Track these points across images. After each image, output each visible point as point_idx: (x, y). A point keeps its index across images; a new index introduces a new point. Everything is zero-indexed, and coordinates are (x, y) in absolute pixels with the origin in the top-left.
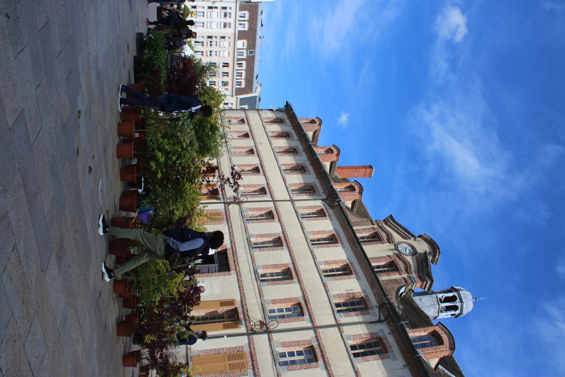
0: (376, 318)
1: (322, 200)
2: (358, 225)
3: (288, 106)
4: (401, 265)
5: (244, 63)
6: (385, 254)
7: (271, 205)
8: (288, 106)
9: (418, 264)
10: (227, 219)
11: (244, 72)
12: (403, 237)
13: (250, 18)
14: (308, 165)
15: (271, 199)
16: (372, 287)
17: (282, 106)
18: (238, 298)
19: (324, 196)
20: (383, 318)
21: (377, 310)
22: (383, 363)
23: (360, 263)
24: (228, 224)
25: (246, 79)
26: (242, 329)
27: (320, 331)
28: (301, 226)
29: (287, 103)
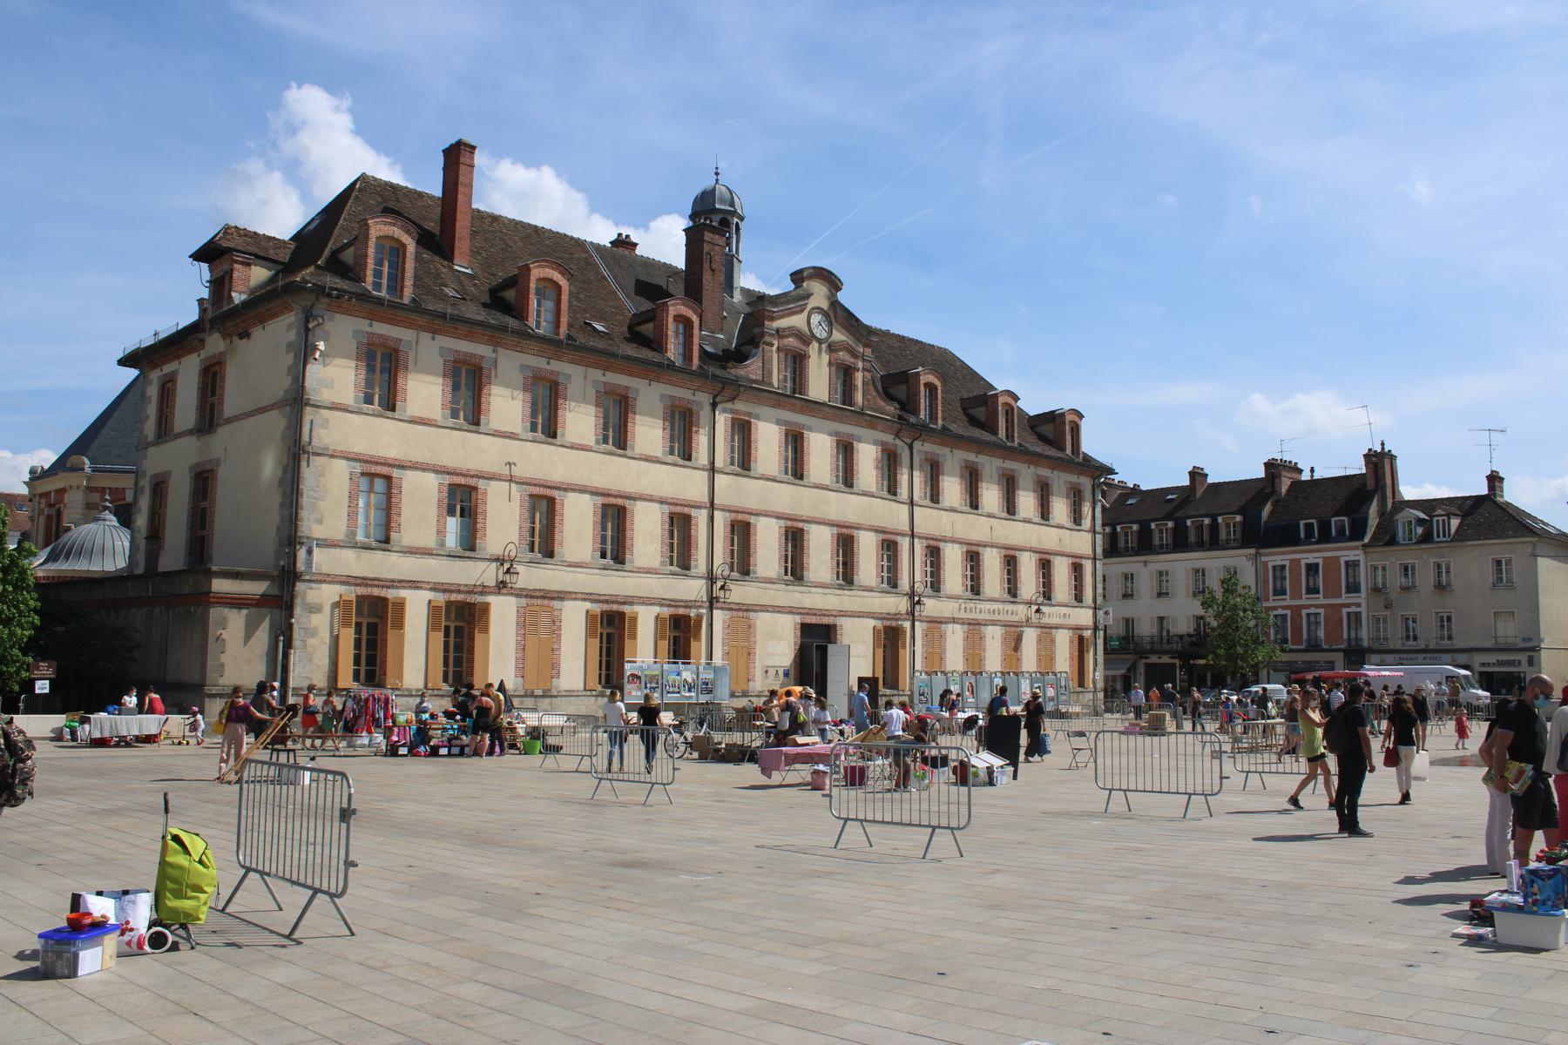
1: (714, 406)
2: (770, 373)
4: (843, 356)
6: (826, 370)
7: (720, 518)
9: (847, 329)
16: (873, 428)
18: (872, 623)
19: (704, 399)
21: (898, 442)
23: (840, 421)
26: (907, 625)
28: (768, 479)
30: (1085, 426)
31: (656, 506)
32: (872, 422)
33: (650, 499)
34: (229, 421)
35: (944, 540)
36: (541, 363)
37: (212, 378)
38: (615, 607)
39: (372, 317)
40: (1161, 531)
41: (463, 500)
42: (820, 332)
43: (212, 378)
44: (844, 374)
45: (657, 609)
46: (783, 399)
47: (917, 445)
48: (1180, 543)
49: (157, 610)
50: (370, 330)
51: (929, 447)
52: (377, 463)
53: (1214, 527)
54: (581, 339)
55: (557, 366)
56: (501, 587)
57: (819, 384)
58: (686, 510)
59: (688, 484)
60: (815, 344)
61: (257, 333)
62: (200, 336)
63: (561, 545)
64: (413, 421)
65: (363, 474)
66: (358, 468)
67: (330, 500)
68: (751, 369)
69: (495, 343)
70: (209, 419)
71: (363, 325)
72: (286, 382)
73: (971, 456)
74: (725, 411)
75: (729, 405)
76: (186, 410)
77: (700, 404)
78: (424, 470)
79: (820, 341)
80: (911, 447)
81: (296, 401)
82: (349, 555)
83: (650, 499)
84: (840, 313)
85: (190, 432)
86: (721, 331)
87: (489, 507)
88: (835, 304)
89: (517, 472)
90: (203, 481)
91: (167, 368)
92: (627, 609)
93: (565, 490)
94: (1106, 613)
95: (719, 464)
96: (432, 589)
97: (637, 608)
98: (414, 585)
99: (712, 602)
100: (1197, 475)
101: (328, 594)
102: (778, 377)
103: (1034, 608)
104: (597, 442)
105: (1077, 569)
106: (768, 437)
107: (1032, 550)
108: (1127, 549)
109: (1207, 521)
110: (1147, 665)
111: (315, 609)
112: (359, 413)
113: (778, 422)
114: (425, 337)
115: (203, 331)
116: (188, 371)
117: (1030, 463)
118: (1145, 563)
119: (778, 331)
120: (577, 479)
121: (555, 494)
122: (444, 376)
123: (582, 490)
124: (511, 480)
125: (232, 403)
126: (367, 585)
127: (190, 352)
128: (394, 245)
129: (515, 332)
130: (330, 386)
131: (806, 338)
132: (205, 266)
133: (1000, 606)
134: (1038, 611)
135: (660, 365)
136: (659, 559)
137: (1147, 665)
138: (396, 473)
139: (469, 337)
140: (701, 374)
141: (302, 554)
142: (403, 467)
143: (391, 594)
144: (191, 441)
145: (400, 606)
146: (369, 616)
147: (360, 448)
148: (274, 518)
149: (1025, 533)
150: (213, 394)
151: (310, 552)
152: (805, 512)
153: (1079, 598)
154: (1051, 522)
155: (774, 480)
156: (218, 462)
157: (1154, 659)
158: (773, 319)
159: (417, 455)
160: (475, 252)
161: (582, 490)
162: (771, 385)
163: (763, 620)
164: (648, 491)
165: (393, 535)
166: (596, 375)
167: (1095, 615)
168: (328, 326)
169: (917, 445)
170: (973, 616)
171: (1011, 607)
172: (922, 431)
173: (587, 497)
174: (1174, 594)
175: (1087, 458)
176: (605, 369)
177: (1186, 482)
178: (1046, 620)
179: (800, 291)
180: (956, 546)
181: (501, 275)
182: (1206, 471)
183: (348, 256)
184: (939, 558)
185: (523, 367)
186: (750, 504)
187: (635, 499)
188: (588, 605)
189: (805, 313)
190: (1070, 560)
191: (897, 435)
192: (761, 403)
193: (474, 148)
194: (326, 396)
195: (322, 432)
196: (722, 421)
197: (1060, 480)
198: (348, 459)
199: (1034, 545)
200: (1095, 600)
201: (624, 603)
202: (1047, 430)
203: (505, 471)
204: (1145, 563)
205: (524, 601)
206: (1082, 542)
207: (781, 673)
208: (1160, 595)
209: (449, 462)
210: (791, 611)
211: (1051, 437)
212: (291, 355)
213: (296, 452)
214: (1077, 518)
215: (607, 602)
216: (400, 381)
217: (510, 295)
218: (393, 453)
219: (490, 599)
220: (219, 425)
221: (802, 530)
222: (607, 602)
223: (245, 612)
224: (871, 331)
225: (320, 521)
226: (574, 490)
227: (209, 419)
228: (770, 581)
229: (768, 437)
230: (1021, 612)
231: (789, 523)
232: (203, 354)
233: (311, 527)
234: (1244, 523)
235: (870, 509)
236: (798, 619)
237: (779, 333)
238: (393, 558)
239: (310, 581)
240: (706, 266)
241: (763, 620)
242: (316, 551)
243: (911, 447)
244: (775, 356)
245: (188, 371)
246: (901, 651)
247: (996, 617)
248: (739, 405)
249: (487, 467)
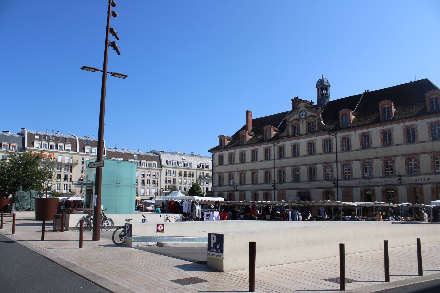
0: (334, 138)
2: (289, 133)
3: (210, 151)
5: (142, 161)
6: (305, 125)
8: (210, 151)
11: (148, 162)
13: (115, 157)
15: (273, 169)
17: (210, 154)
18: (322, 190)
20: (334, 135)
21: (331, 136)
25: (152, 161)
27: (338, 160)
29: (209, 151)
33: (261, 169)
35: (352, 161)
45: (263, 192)
56: (237, 191)
60: (301, 120)
68: (285, 134)
73: (365, 131)
77: (271, 147)
80: (336, 136)
89: (239, 170)
107: (401, 155)
124: (237, 171)
131: (298, 120)
155: (290, 158)
158: (289, 120)
163: (288, 192)
180: (358, 162)
189: (298, 114)
191: (329, 135)
236: (297, 191)
243: (336, 136)
249: (234, 170)
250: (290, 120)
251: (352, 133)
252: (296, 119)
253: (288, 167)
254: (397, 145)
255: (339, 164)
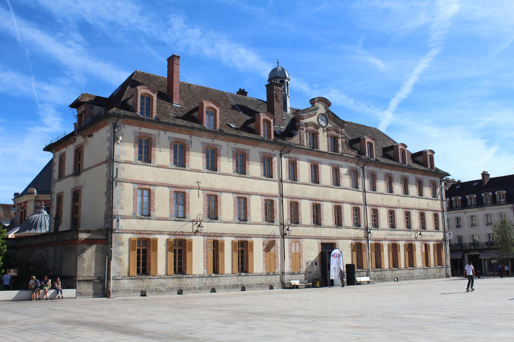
1: (281, 155)
2: (303, 141)
4: (334, 133)
10: (298, 238)
12: (315, 115)
14: (235, 146)
16: (347, 161)
19: (277, 152)
21: (358, 167)
22: (380, 180)
24: (302, 238)
28: (305, 184)
30: (435, 156)
31: (259, 197)
32: (347, 159)
34: (86, 170)
36: (209, 141)
37: (79, 154)
38: (244, 239)
39: (140, 126)
40: (471, 199)
41: (180, 197)
42: (323, 124)
43: (79, 154)
44: (334, 141)
46: (309, 151)
47: (366, 168)
48: (480, 204)
49: (58, 247)
50: (140, 131)
51: (371, 168)
52: (144, 184)
53: (494, 196)
54: (226, 131)
55: (216, 142)
57: (324, 144)
58: (271, 198)
59: (271, 187)
60: (321, 129)
61: (95, 134)
62: (74, 137)
63: (221, 214)
64: (158, 167)
65: (139, 189)
66: (137, 186)
67: (125, 200)
68: (295, 140)
69: (191, 134)
70: (78, 170)
71: (137, 129)
72: (107, 154)
73: (388, 171)
74: (285, 157)
75: (287, 155)
76: (69, 168)
78: (163, 186)
79: (323, 127)
80: (363, 168)
81: (111, 160)
82: (134, 221)
83: (256, 194)
84: (331, 115)
85: (71, 175)
86: (283, 125)
87: (191, 200)
88: (328, 111)
89: (201, 185)
90: (76, 195)
91: (62, 151)
92: (249, 240)
93: (221, 192)
94: (450, 234)
95: (284, 179)
96: (168, 234)
97: (253, 239)
98: (161, 233)
99: (283, 235)
100: (485, 175)
101: (126, 237)
102: (306, 143)
103: (419, 233)
104: (234, 172)
105: (436, 216)
106: (304, 168)
108: (472, 205)
109: (491, 194)
110: (469, 255)
111: (121, 244)
112: (136, 164)
113: (308, 161)
114: (162, 133)
115: (75, 135)
116: (70, 151)
117: (413, 173)
118: (465, 212)
119: (306, 124)
120: (226, 188)
121: (217, 194)
122: (171, 148)
123: (228, 192)
125: (86, 164)
126: (142, 234)
127: (70, 144)
128: (149, 96)
129: (199, 129)
130: (124, 154)
132: (75, 110)
133: (404, 232)
134: (420, 234)
135: (258, 140)
136: (261, 218)
137: (469, 255)
138: (152, 188)
139: (179, 132)
140: (275, 142)
141: (115, 221)
142: (155, 185)
143: (151, 237)
144: (72, 179)
145: (155, 241)
146: (143, 246)
147: (138, 178)
148: (104, 208)
149: (412, 201)
150: (80, 160)
151: (118, 221)
152: (321, 197)
153: (437, 228)
154: (424, 197)
156: (82, 186)
157: (472, 253)
158: (303, 119)
159: (160, 180)
160: (182, 98)
161: (228, 192)
162: (304, 146)
164: (256, 191)
165: (152, 213)
166: (232, 145)
167: (445, 236)
168: (123, 130)
169: (366, 168)
170: (393, 237)
171: (408, 233)
172: (368, 162)
173: (230, 194)
174: (480, 224)
175: (437, 170)
176: (236, 142)
177: (480, 178)
178: (424, 238)
179: (314, 108)
180: (384, 209)
181: (193, 107)
182: (489, 173)
183: (130, 102)
184: (377, 214)
185: (202, 143)
186: (298, 194)
187: (250, 194)
188: (233, 239)
189: (316, 116)
190: (433, 212)
191: (357, 164)
192: (300, 153)
193: (179, 57)
194: (123, 158)
195: (122, 172)
196: (285, 161)
197: (426, 179)
198: (133, 183)
199: (417, 206)
200: (444, 229)
201: (247, 237)
202: (420, 159)
203: (197, 185)
204: (465, 212)
205: (206, 238)
206: (436, 205)
207: (314, 264)
208: (472, 226)
209: (174, 182)
210: (317, 238)
211: (422, 162)
212: (109, 142)
213: (111, 182)
214: (434, 195)
215: (240, 237)
216: (153, 152)
217: (196, 114)
218: (151, 180)
219: (194, 238)
220: (82, 172)
221: (320, 204)
222: (240, 237)
223: (94, 247)
224: (344, 122)
225: (122, 209)
226: (225, 192)
227: (78, 170)
228: (307, 226)
229: (304, 168)
230: (413, 234)
231: (314, 202)
232: (75, 144)
233: (117, 211)
234: (507, 194)
235: (347, 195)
236: (320, 241)
237: (306, 125)
238: (153, 222)
239: (118, 233)
240: (275, 99)
241: (305, 242)
242: (120, 220)
243: (363, 168)
244: (305, 134)
245: (70, 151)
246: (364, 253)
247: (402, 237)
248: (291, 155)
249: (189, 184)
250: (305, 121)
251: (377, 169)
252: (314, 125)
253: (305, 199)
254: (412, 197)
255: (367, 207)
